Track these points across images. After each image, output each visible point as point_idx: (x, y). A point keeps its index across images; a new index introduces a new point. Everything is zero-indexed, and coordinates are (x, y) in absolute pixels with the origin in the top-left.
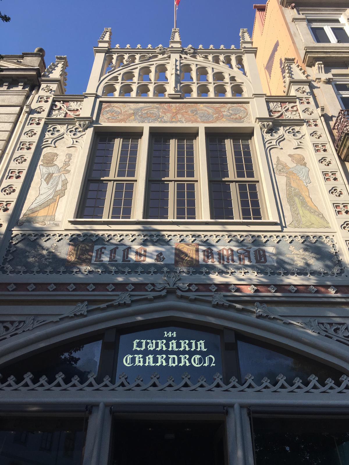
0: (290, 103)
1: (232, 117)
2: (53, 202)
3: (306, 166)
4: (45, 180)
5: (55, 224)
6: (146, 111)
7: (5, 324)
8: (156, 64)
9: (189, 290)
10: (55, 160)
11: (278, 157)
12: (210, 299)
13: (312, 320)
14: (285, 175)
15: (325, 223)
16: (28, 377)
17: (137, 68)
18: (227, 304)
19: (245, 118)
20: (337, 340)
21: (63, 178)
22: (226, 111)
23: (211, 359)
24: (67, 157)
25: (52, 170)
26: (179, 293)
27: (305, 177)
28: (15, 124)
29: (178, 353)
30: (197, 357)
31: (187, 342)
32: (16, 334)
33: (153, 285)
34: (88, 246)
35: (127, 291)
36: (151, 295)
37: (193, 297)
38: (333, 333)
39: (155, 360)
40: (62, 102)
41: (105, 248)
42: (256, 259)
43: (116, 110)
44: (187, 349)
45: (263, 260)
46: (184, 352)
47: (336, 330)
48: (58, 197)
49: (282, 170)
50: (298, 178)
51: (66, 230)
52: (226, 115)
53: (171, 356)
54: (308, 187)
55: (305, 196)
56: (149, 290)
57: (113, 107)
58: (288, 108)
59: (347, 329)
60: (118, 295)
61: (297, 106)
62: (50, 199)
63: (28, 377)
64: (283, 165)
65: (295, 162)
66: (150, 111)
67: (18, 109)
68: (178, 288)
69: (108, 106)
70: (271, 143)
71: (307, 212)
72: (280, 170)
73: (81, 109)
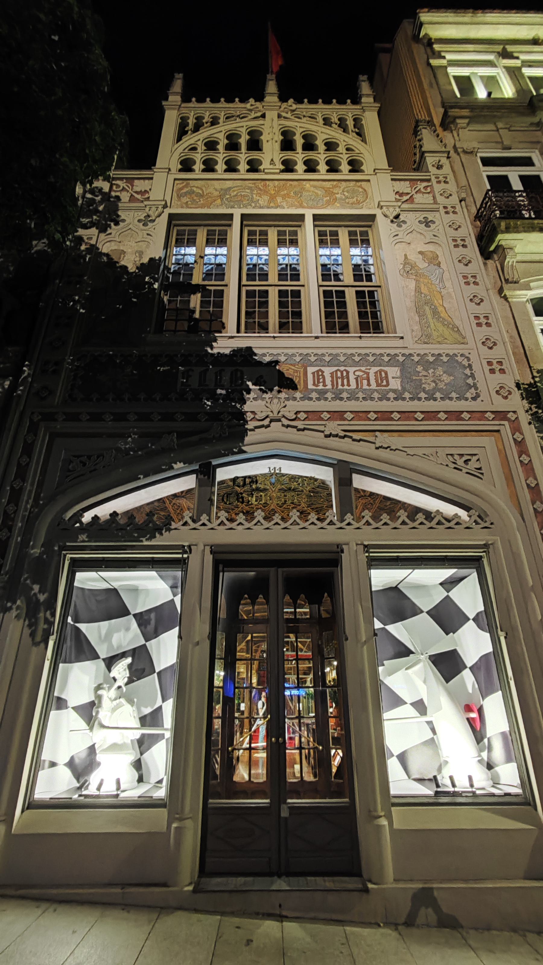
1: (347, 200)
3: (440, 266)
6: (235, 193)
7: (82, 459)
10: (121, 259)
11: (405, 255)
12: (321, 428)
13: (438, 450)
14: (414, 277)
15: (460, 339)
17: (221, 131)
18: (342, 434)
19: (364, 203)
20: (467, 473)
22: (340, 192)
24: (137, 255)
26: (286, 422)
27: (438, 280)
37: (301, 427)
38: (463, 465)
40: (125, 181)
42: (377, 381)
45: (385, 383)
47: (466, 462)
49: (410, 272)
52: (341, 199)
54: (443, 294)
55: (438, 305)
57: (193, 187)
59: (478, 460)
61: (431, 186)
64: (412, 266)
68: (284, 416)
69: (186, 186)
70: (397, 235)
71: (440, 324)
72: (408, 272)
73: (150, 190)
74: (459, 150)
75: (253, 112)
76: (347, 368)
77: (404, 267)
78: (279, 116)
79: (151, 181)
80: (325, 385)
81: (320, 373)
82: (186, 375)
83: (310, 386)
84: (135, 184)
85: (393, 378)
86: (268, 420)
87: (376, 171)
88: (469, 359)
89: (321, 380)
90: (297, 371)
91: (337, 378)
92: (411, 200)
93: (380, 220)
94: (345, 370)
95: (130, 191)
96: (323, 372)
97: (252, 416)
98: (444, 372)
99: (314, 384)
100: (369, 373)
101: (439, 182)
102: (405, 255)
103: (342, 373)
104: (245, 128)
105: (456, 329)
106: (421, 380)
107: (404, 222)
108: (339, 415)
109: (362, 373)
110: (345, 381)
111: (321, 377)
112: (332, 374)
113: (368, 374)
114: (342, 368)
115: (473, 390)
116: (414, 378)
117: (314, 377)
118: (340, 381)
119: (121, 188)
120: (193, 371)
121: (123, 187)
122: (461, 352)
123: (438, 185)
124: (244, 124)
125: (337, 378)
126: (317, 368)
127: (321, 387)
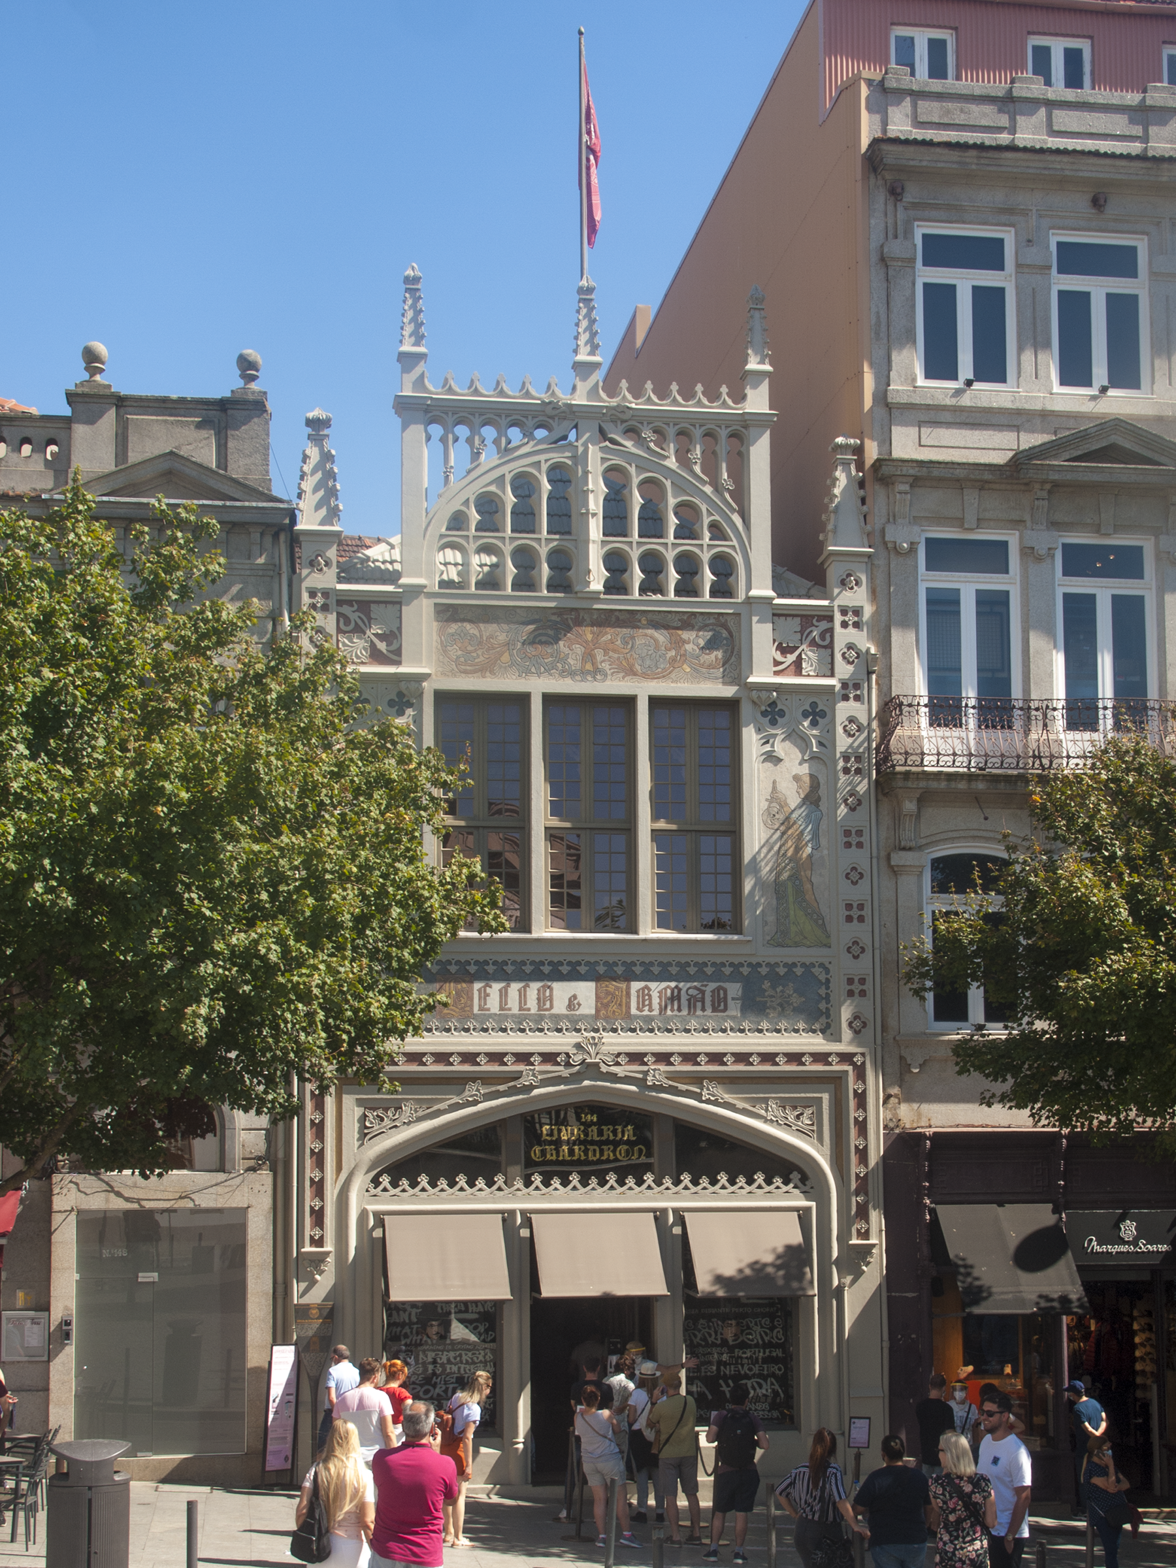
0: (821, 618)
3: (818, 806)
8: (546, 461)
9: (618, 1064)
11: (774, 782)
12: (640, 1076)
16: (424, 1180)
23: (640, 1151)
26: (604, 1069)
29: (600, 1144)
30: (626, 1147)
31: (611, 1128)
32: (396, 1127)
33: (567, 1054)
36: (565, 1072)
39: (571, 1152)
43: (471, 631)
44: (612, 1138)
45: (722, 1007)
46: (608, 1142)
47: (798, 1117)
53: (591, 1148)
55: (804, 879)
61: (831, 630)
63: (424, 1180)
66: (540, 635)
73: (400, 629)
74: (890, 545)
77: (769, 807)
80: (651, 1010)
82: (484, 996)
83: (634, 1011)
85: (733, 999)
88: (827, 971)
96: (649, 990)
98: (795, 991)
99: (638, 1009)
102: (774, 782)
105: (820, 922)
106: (766, 1002)
108: (664, 1057)
113: (703, 992)
114: (673, 984)
115: (823, 1020)
116: (758, 999)
117: (638, 997)
119: (353, 625)
122: (821, 960)
123: (843, 630)
124: (542, 457)
126: (642, 984)
127: (646, 1013)
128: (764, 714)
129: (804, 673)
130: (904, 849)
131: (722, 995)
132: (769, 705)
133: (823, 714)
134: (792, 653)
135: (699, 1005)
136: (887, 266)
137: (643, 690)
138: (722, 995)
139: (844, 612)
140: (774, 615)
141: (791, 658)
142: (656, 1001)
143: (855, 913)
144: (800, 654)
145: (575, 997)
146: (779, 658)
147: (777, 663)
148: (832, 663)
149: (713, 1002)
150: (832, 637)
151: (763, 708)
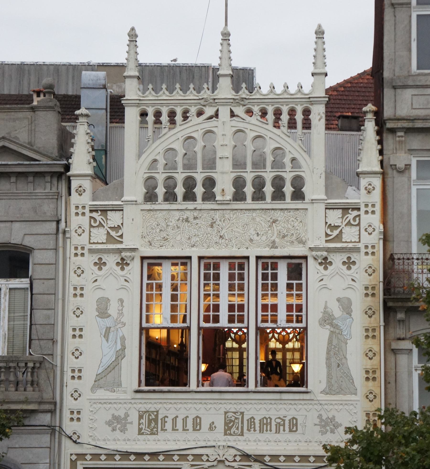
0: (353, 209)
2: (116, 366)
3: (351, 315)
4: (104, 336)
5: (123, 391)
9: (235, 461)
10: (108, 309)
11: (326, 302)
21: (121, 335)
24: (120, 302)
25: (108, 322)
26: (227, 463)
27: (347, 331)
28: (56, 249)
33: (207, 455)
34: (154, 414)
35: (188, 461)
40: (100, 213)
41: (167, 417)
42: (290, 428)
45: (295, 429)
48: (120, 357)
49: (327, 322)
50: (340, 333)
51: (132, 399)
56: (205, 460)
58: (350, 220)
60: (182, 465)
61: (360, 215)
62: (113, 362)
65: (342, 310)
67: (54, 224)
70: (322, 280)
73: (122, 224)
75: (207, 107)
76: (271, 417)
78: (233, 114)
79: (121, 212)
81: (252, 420)
84: (108, 218)
86: (216, 462)
87: (313, 201)
89: (253, 426)
90: (236, 418)
91: (264, 424)
92: (339, 238)
93: (310, 261)
94: (269, 418)
95: (105, 225)
96: (254, 419)
97: (207, 458)
100: (285, 420)
101: (367, 212)
102: (326, 302)
103: (267, 419)
104: (201, 132)
105: (351, 381)
107: (331, 263)
109: (280, 421)
110: (269, 426)
111: (252, 423)
112: (260, 420)
113: (284, 421)
118: (265, 426)
119: (98, 223)
120: (167, 417)
121: (100, 222)
125: (264, 424)
128: (321, 264)
129: (343, 240)
130: (399, 339)
131: (295, 423)
132: (324, 259)
133: (354, 263)
134: (336, 230)
135: (282, 428)
136: (394, 8)
137: (252, 253)
138: (295, 423)
139: (366, 206)
140: (326, 208)
141: (336, 232)
142: (257, 425)
143: (371, 376)
144: (341, 230)
145: (213, 423)
146: (329, 232)
147: (327, 235)
148: (360, 235)
149: (290, 425)
150: (359, 219)
151: (320, 261)
